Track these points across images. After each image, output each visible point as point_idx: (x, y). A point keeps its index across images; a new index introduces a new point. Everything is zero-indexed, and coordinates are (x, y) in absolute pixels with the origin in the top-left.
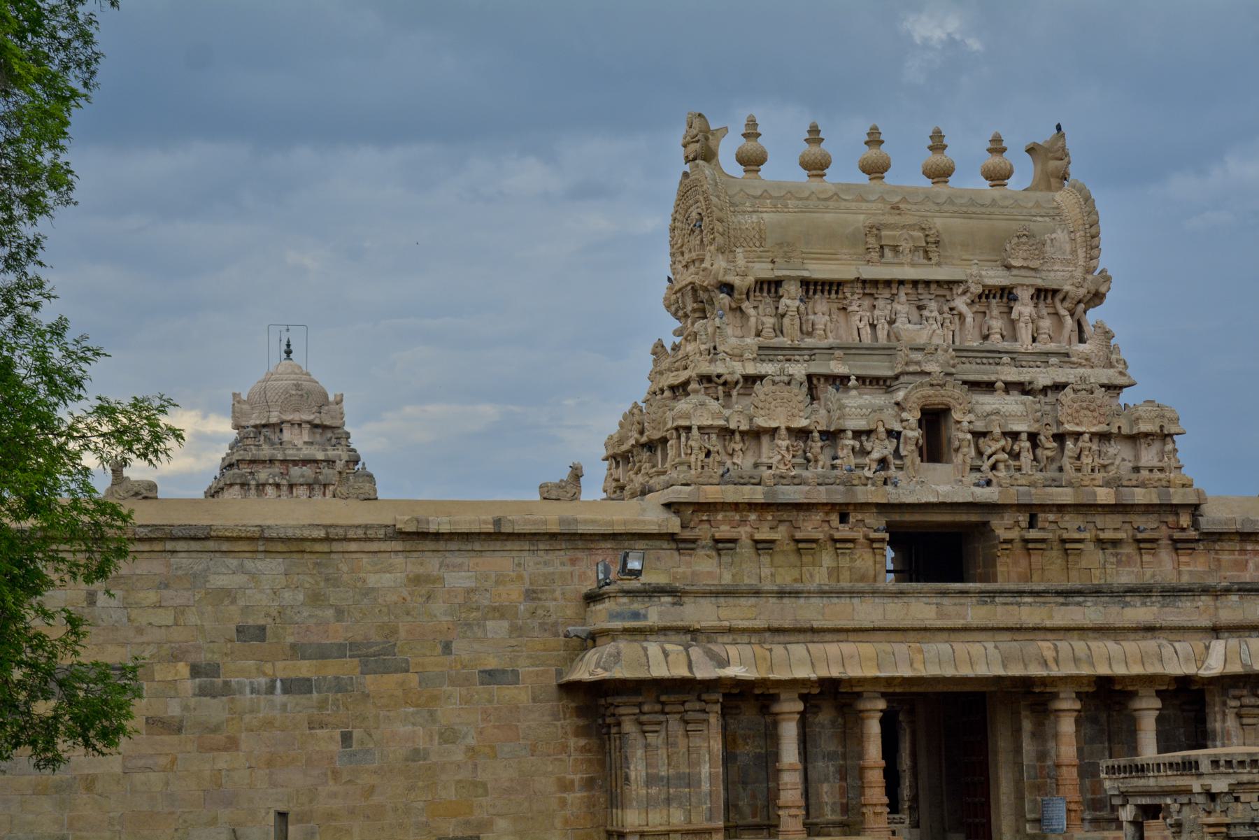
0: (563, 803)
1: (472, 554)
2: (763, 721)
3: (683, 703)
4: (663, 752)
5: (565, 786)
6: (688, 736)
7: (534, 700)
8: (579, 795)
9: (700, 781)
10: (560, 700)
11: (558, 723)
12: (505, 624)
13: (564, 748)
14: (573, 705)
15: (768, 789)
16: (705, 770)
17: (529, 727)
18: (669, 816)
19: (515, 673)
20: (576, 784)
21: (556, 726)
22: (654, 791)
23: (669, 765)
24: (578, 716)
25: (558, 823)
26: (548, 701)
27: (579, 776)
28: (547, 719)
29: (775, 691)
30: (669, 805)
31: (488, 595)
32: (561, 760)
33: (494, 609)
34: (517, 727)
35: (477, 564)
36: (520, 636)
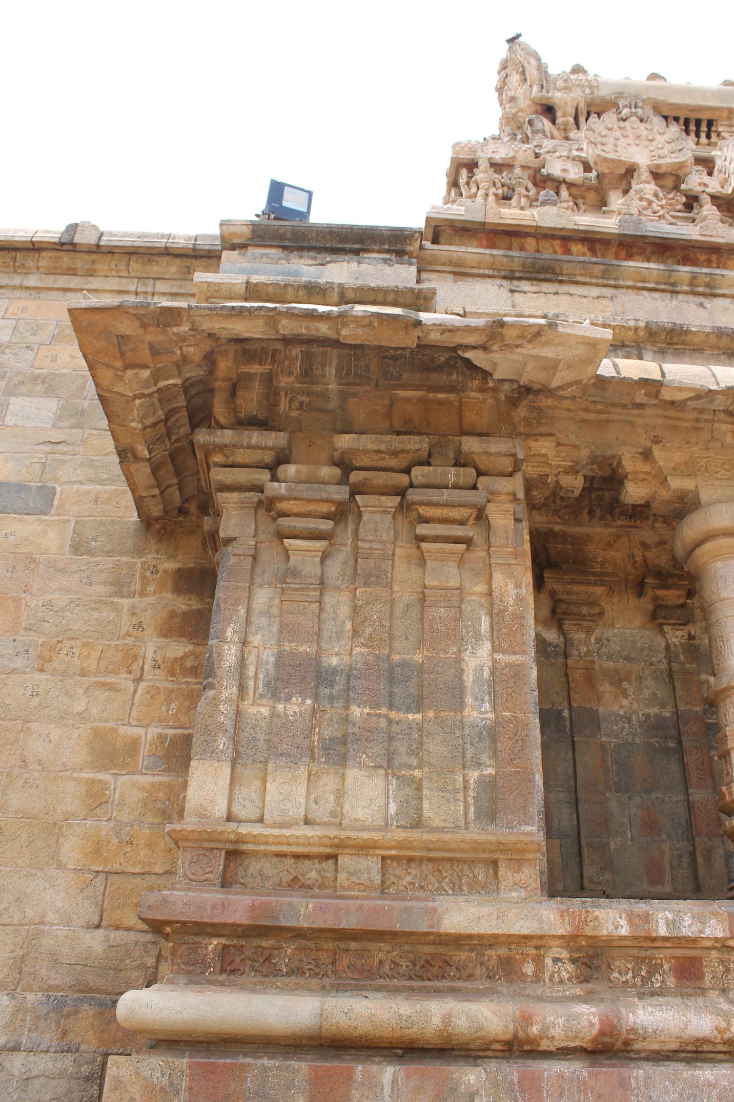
0: (97, 798)
1: (18, 293)
2: (660, 642)
3: (407, 471)
4: (339, 604)
5: (110, 753)
6: (422, 562)
7: (76, 548)
8: (146, 780)
9: (457, 692)
10: (139, 552)
11: (126, 602)
12: (51, 405)
13: (129, 659)
14: (171, 565)
15: (690, 807)
16: (478, 659)
17: (49, 605)
18: (340, 795)
19: (47, 494)
20: (144, 750)
21: (117, 609)
22: (296, 707)
23: (355, 633)
24: (178, 590)
25: (71, 850)
26: (109, 553)
27: (154, 731)
28: (99, 590)
29: (687, 484)
30: (343, 760)
31: (30, 355)
32: (111, 687)
33: (36, 379)
34: (17, 601)
35: (24, 310)
36: (77, 426)
